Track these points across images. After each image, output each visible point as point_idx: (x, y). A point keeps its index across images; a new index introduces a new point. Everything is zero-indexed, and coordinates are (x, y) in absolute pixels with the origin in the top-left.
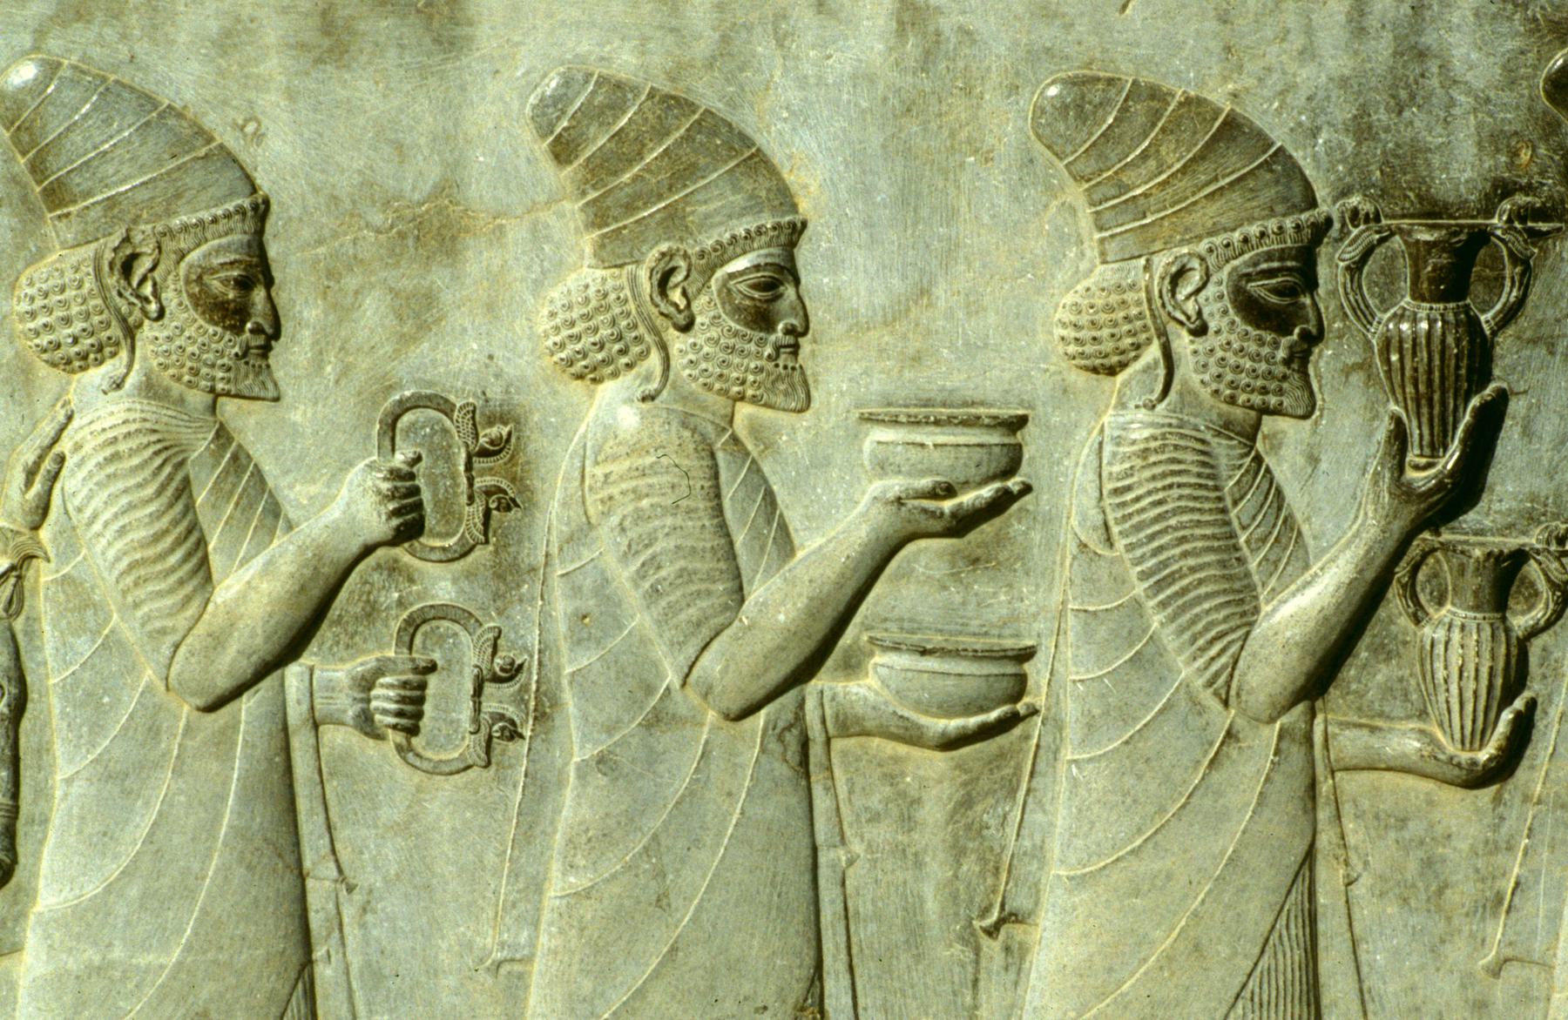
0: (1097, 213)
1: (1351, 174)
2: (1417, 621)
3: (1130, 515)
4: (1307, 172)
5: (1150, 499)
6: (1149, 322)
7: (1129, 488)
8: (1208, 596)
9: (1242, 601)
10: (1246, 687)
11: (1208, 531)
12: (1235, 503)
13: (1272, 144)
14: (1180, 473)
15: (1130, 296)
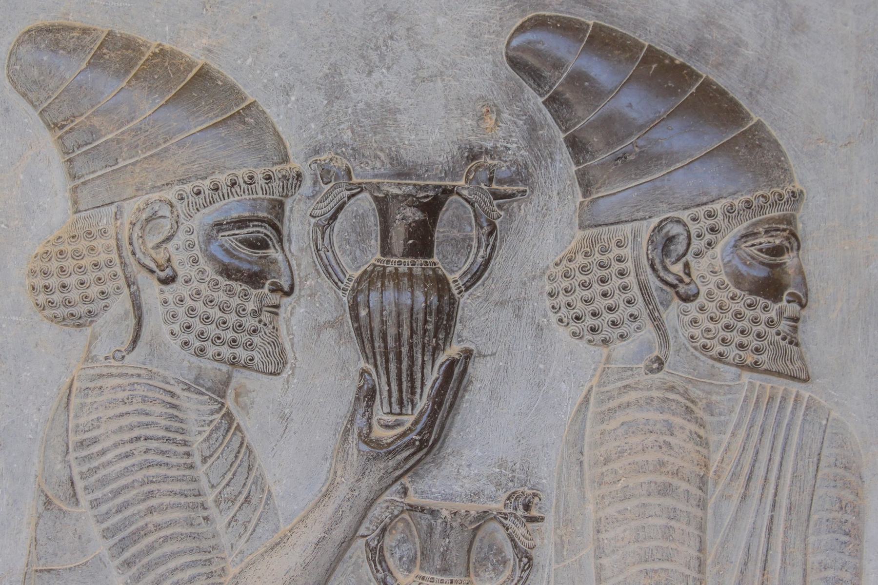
1: (322, 132)
4: (280, 129)
5: (117, 452)
6: (118, 269)
7: (95, 441)
11: (177, 487)
12: (205, 460)
13: (244, 99)
15: (99, 243)
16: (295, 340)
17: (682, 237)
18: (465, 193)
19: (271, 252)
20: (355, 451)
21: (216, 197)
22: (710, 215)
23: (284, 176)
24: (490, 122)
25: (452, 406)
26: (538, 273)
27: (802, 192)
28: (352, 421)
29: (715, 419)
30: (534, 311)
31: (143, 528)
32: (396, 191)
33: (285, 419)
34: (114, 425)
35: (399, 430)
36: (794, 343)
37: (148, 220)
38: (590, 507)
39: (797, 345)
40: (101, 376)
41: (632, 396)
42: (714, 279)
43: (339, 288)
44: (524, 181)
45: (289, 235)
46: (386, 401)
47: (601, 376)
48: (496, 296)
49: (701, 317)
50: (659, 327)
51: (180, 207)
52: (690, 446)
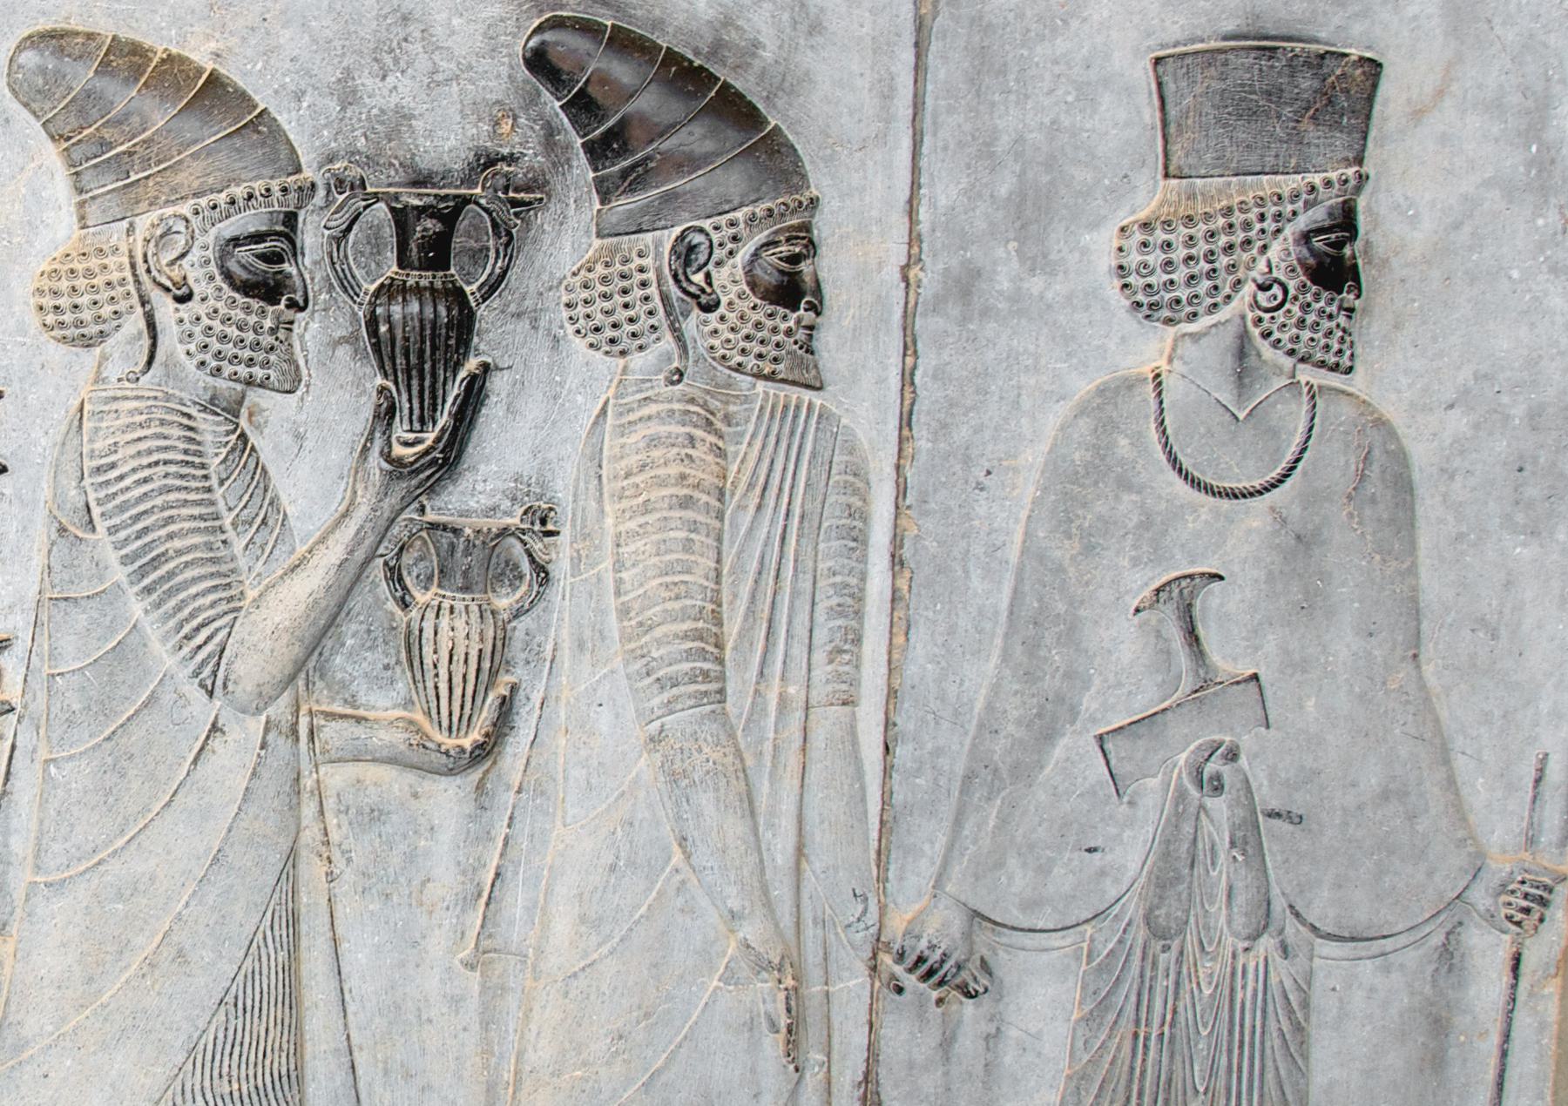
1: (336, 140)
2: (405, 605)
3: (115, 494)
4: (292, 137)
6: (131, 288)
7: (113, 466)
8: (195, 580)
9: (229, 585)
10: (232, 677)
11: (196, 511)
12: (222, 483)
13: (255, 107)
14: (166, 448)
15: (110, 261)
16: (310, 357)
17: (703, 247)
18: (483, 201)
19: (286, 266)
20: (377, 472)
21: (232, 210)
22: (732, 224)
23: (300, 188)
24: (506, 127)
26: (555, 284)
27: (818, 199)
29: (731, 430)
30: (550, 322)
31: (163, 554)
32: (416, 202)
33: (299, 437)
34: (132, 450)
35: (420, 448)
36: (810, 351)
37: (162, 236)
38: (609, 521)
39: (812, 353)
40: (115, 399)
41: (652, 409)
42: (735, 289)
43: (355, 302)
44: (541, 188)
45: (302, 248)
46: (406, 419)
47: (618, 387)
49: (721, 327)
50: (679, 339)
52: (710, 458)
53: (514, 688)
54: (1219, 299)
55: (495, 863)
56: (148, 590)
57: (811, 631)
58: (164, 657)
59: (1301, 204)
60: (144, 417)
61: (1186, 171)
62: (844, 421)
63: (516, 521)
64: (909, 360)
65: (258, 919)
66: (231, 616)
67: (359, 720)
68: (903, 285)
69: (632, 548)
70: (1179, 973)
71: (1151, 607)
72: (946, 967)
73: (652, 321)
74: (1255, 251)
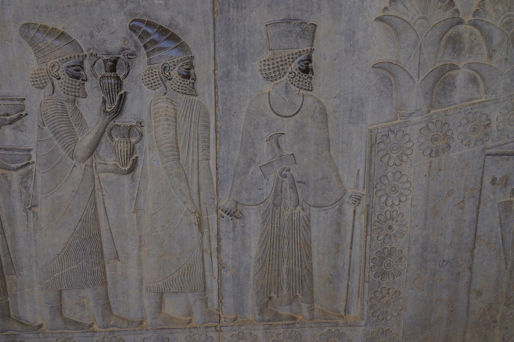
0: (35, 53)
3: (48, 119)
4: (81, 45)
6: (48, 77)
7: (47, 113)
8: (66, 137)
9: (74, 137)
10: (76, 156)
11: (65, 122)
12: (71, 116)
14: (58, 110)
18: (122, 58)
22: (174, 62)
24: (126, 42)
25: (123, 104)
28: (101, 108)
31: (59, 131)
34: (51, 110)
38: (153, 124)
41: (160, 100)
42: (175, 75)
48: (131, 80)
49: (173, 83)
50: (165, 86)
51: (60, 63)
52: (172, 111)
53: (137, 157)
54: (281, 76)
55: (137, 192)
56: (57, 138)
57: (198, 145)
58: (62, 152)
59: (298, 55)
60: (52, 103)
61: (273, 49)
62: (203, 103)
63: (135, 124)
64: (216, 90)
65: (87, 204)
66: (75, 143)
67: (105, 164)
68: (214, 74)
69: (157, 129)
70: (280, 214)
71: (269, 140)
72: (232, 212)
73: (159, 82)
74: (288, 66)
